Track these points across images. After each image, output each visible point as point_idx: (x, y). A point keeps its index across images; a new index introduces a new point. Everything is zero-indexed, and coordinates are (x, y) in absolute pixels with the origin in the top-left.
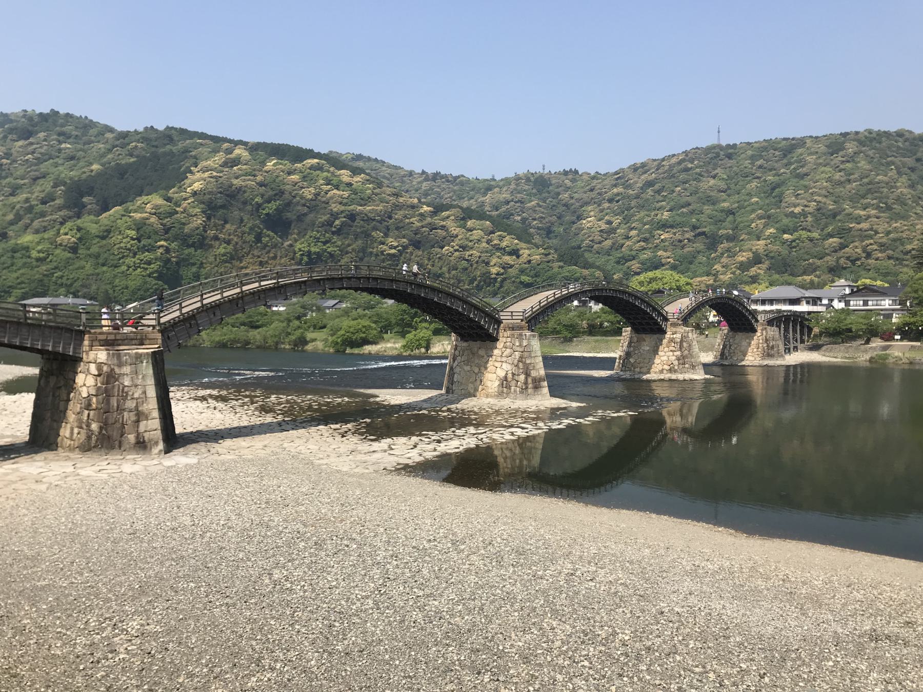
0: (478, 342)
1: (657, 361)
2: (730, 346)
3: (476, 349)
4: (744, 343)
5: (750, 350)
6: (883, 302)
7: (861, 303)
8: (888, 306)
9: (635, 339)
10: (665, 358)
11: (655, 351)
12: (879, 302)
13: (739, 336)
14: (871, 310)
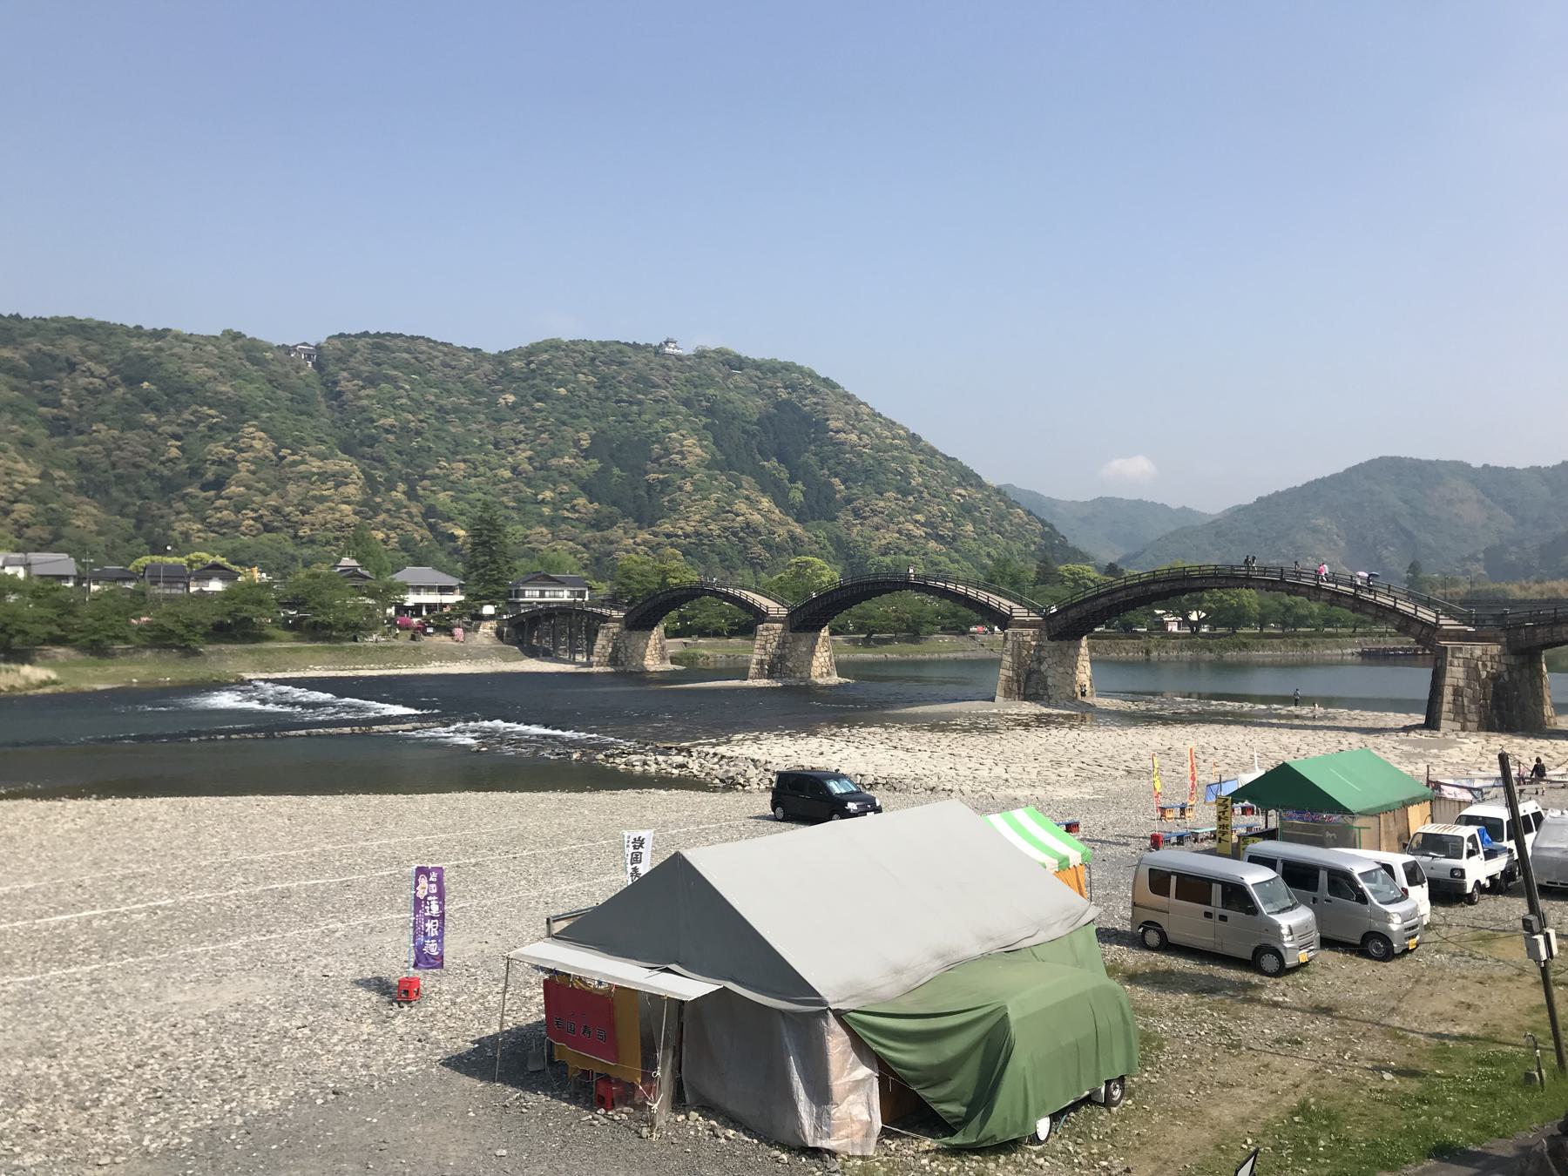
0: (1066, 643)
1: (815, 663)
2: (626, 648)
3: (1065, 649)
4: (642, 644)
5: (648, 653)
6: (561, 594)
7: (538, 593)
8: (566, 599)
9: (790, 639)
10: (822, 660)
11: (812, 652)
12: (557, 593)
13: (636, 635)
14: (549, 603)
